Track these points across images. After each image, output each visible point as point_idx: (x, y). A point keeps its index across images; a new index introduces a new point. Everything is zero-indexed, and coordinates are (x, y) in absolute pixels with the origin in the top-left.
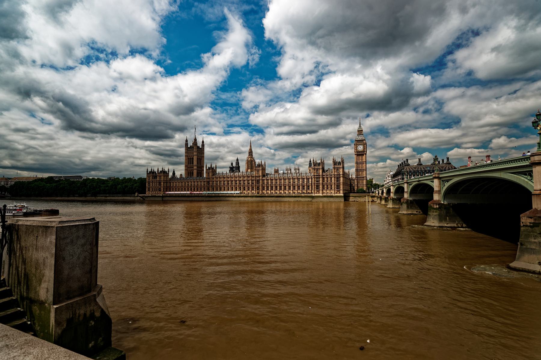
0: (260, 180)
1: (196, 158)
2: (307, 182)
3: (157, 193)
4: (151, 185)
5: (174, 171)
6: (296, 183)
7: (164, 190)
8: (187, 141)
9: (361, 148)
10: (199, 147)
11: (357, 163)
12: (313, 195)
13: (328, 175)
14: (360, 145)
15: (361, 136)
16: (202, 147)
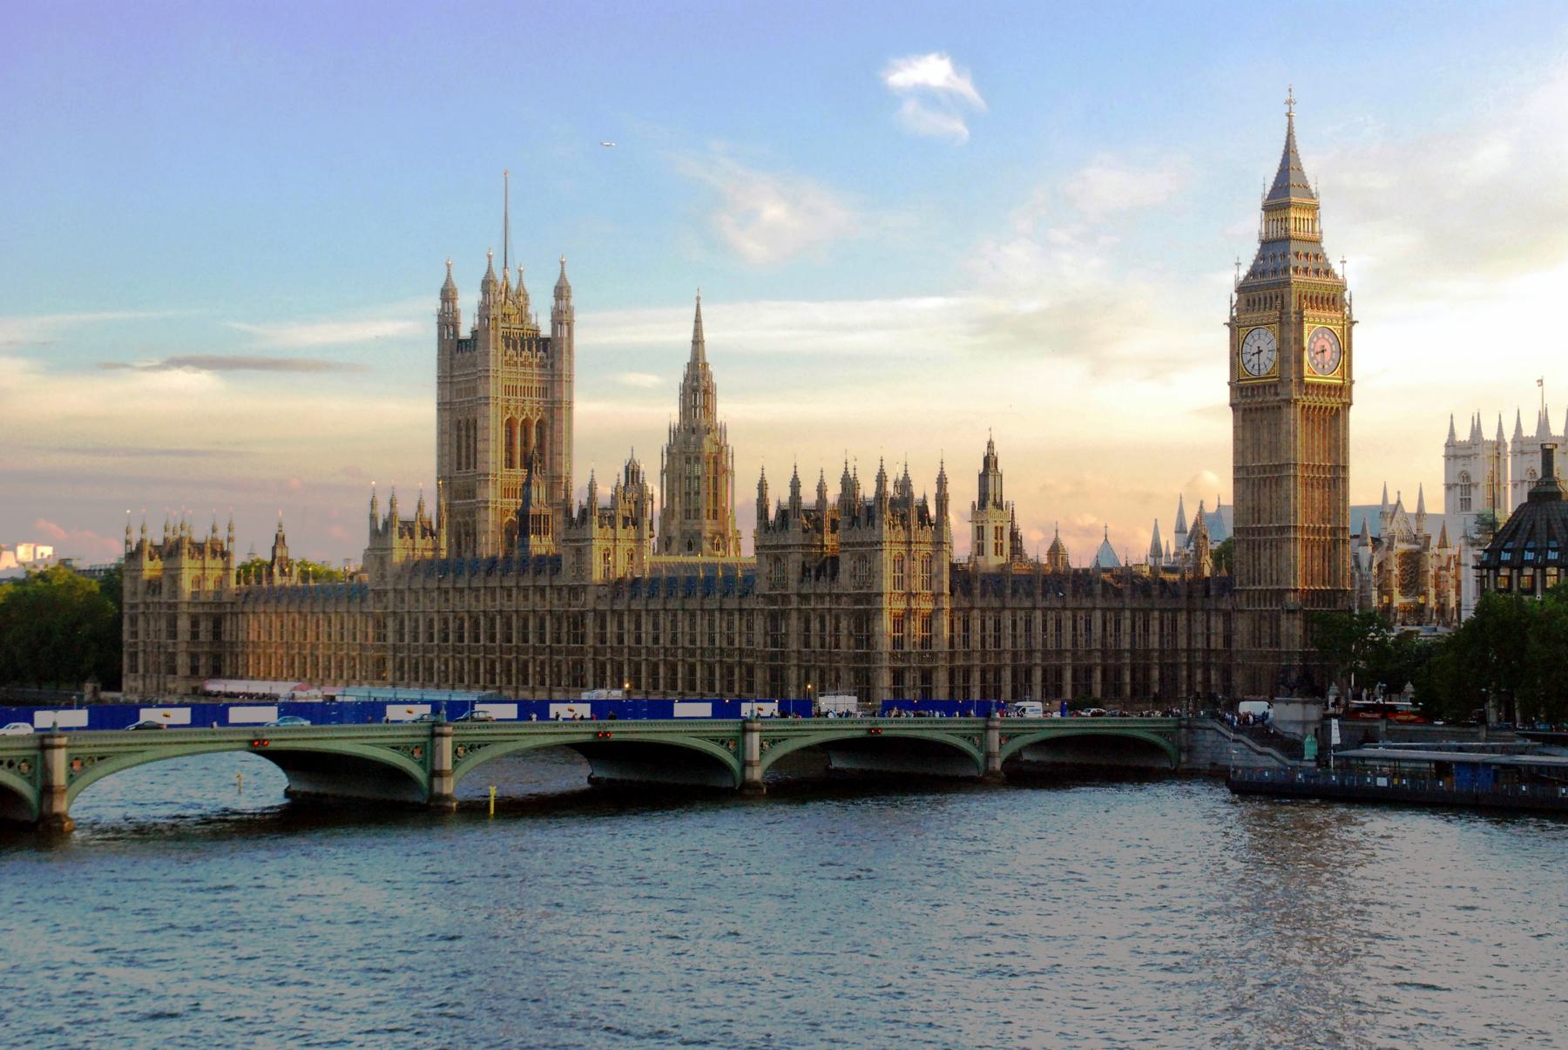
0: (583, 614)
7: (194, 670)
8: (448, 295)
10: (537, 331)
13: (821, 597)
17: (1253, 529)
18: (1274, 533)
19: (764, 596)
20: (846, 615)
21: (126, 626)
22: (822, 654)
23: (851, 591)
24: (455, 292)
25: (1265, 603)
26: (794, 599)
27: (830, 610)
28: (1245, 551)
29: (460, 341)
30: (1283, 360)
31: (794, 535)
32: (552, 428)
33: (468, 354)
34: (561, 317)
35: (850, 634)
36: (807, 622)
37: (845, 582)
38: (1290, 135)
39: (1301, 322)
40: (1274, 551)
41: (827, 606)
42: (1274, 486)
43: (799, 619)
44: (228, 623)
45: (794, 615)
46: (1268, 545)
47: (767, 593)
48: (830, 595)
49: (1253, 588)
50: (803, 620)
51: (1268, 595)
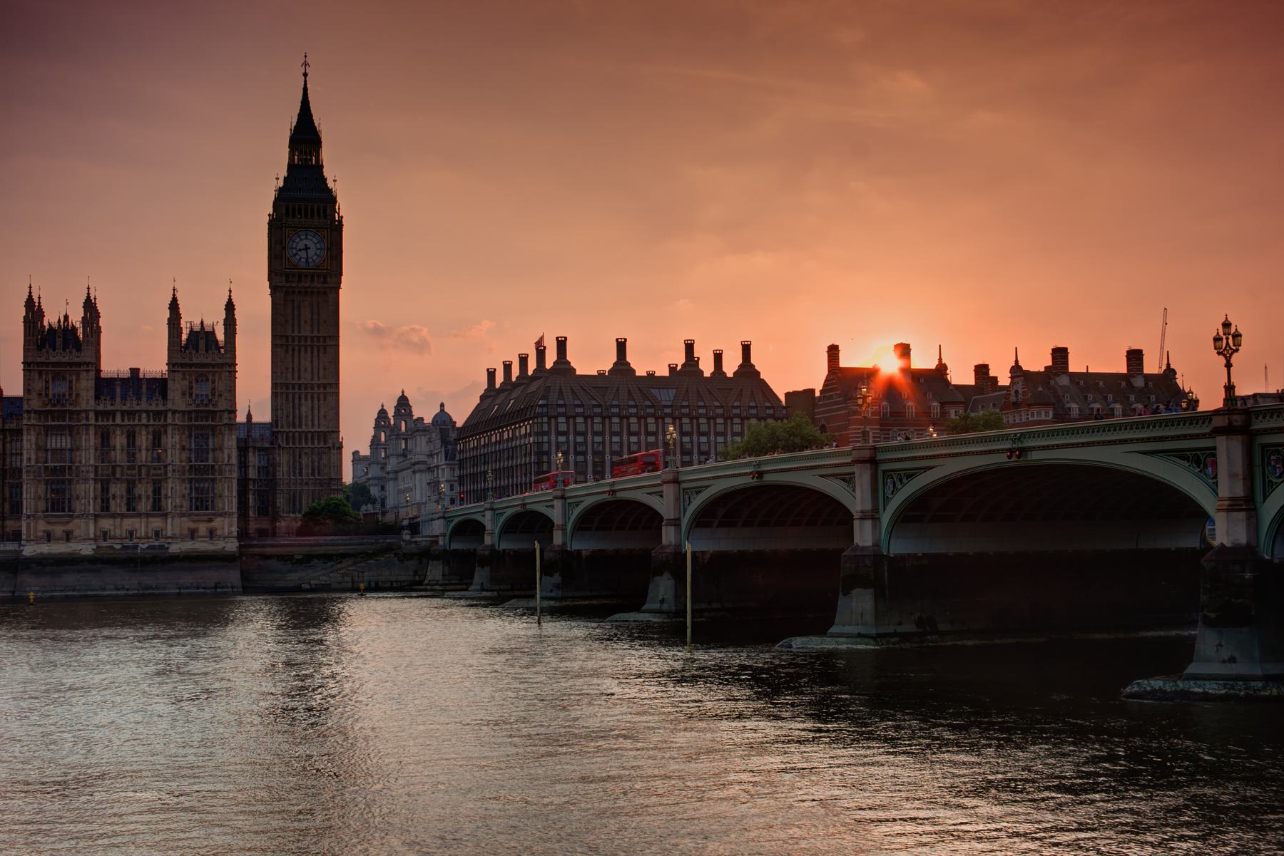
12: (29, 550)
13: (131, 414)
17: (294, 385)
18: (316, 390)
19: (36, 412)
20: (179, 430)
22: (129, 468)
23: (183, 408)
25: (306, 439)
26: (92, 415)
27: (147, 426)
28: (284, 401)
35: (183, 448)
37: (177, 399)
38: (305, 89)
40: (316, 402)
41: (144, 421)
43: (96, 433)
47: (44, 409)
48: (147, 412)
49: (294, 430)
50: (99, 435)
51: (310, 436)
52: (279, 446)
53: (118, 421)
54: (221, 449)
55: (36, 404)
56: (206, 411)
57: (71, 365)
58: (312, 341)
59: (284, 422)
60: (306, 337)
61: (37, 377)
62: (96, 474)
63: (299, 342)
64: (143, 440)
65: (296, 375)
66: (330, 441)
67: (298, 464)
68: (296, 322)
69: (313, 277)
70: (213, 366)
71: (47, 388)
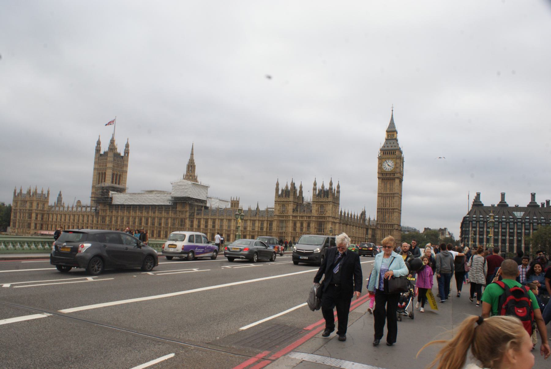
0: (185, 219)
1: (111, 174)
2: (267, 229)
3: (24, 230)
4: (18, 218)
5: (60, 195)
6: (248, 229)
7: (36, 228)
8: (99, 143)
9: (389, 165)
10: (120, 154)
11: (381, 195)
13: (302, 217)
14: (389, 159)
15: (392, 142)
16: (125, 153)
17: (383, 209)
18: (390, 210)
19: (277, 215)
21: (12, 214)
23: (316, 215)
24: (100, 142)
26: (291, 217)
27: (306, 221)
28: (380, 214)
29: (101, 154)
30: (396, 168)
31: (291, 199)
32: (122, 177)
33: (104, 157)
34: (127, 152)
35: (315, 228)
36: (295, 224)
37: (314, 213)
38: (392, 115)
39: (400, 159)
40: (390, 214)
41: (305, 219)
42: (391, 199)
43: (292, 223)
44: (46, 216)
45: (291, 222)
46: (388, 212)
48: (306, 216)
51: (388, 225)
52: (378, 228)
53: (298, 219)
54: (326, 229)
55: (277, 213)
56: (322, 217)
57: (287, 202)
58: (390, 195)
59: (380, 221)
60: (388, 194)
61: (278, 204)
62: (292, 234)
63: (386, 195)
64: (305, 225)
65: (384, 205)
66: (394, 227)
67: (383, 234)
68: (385, 189)
69: (390, 174)
70: (325, 202)
71: (280, 209)
